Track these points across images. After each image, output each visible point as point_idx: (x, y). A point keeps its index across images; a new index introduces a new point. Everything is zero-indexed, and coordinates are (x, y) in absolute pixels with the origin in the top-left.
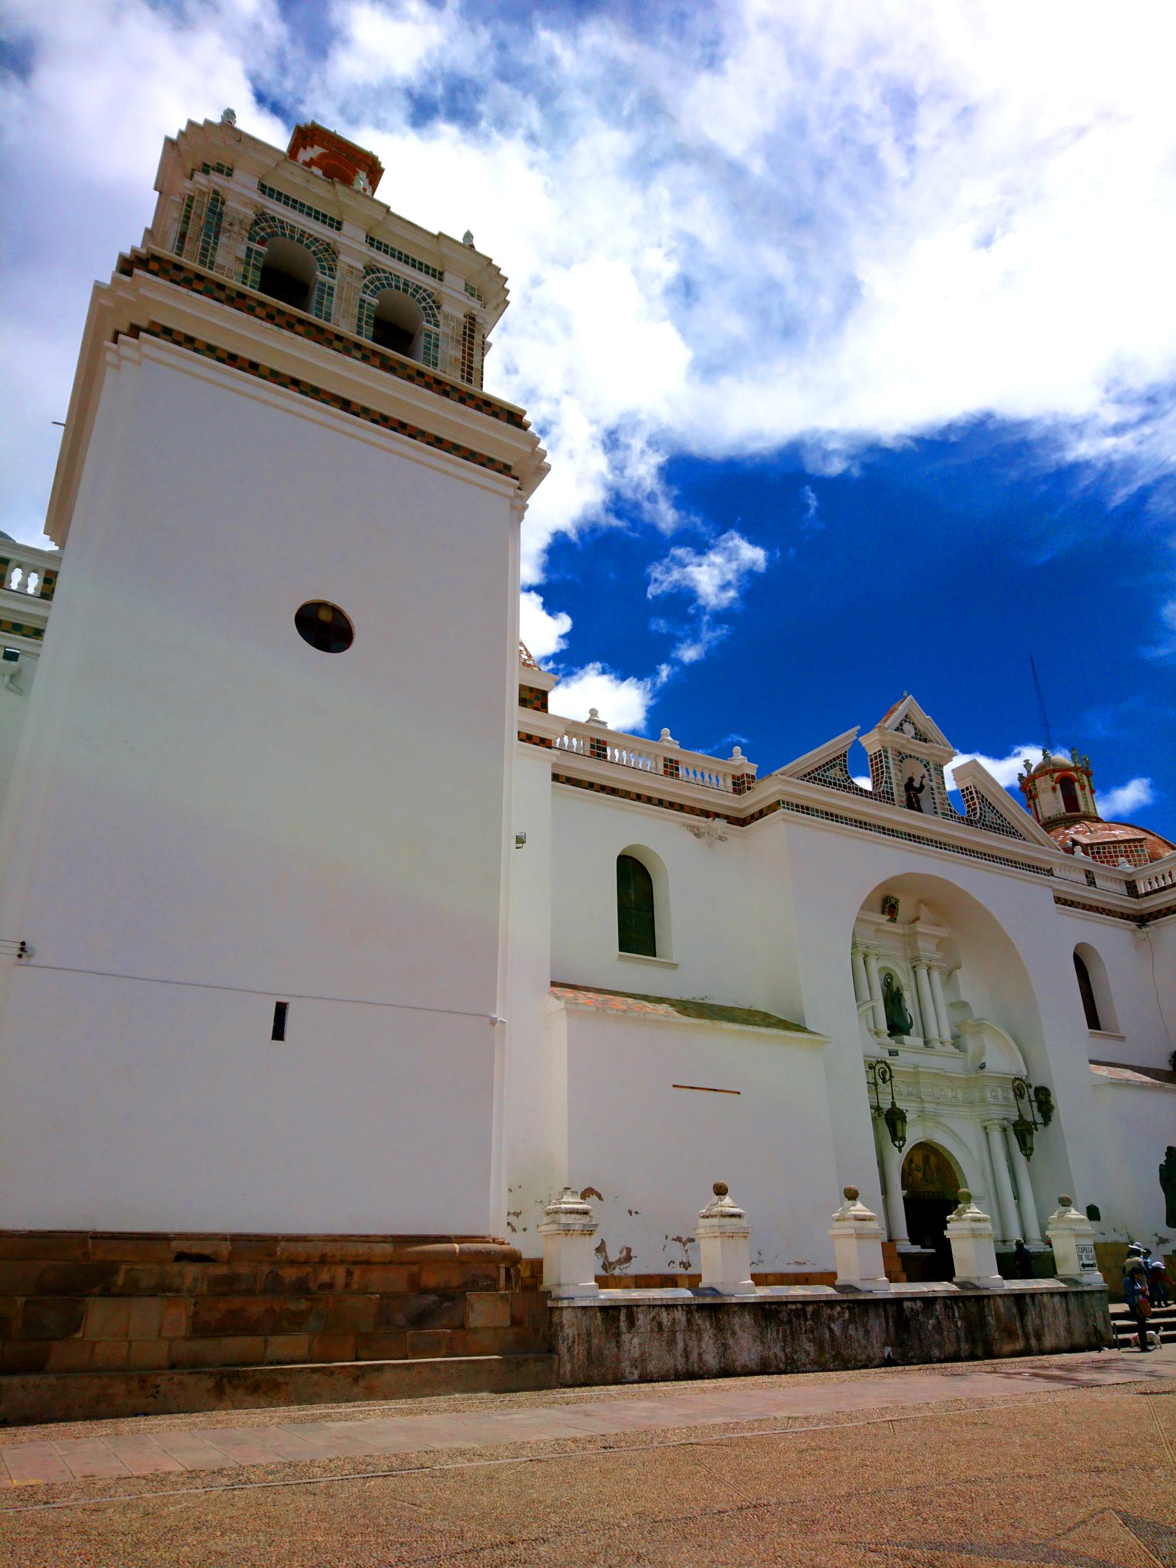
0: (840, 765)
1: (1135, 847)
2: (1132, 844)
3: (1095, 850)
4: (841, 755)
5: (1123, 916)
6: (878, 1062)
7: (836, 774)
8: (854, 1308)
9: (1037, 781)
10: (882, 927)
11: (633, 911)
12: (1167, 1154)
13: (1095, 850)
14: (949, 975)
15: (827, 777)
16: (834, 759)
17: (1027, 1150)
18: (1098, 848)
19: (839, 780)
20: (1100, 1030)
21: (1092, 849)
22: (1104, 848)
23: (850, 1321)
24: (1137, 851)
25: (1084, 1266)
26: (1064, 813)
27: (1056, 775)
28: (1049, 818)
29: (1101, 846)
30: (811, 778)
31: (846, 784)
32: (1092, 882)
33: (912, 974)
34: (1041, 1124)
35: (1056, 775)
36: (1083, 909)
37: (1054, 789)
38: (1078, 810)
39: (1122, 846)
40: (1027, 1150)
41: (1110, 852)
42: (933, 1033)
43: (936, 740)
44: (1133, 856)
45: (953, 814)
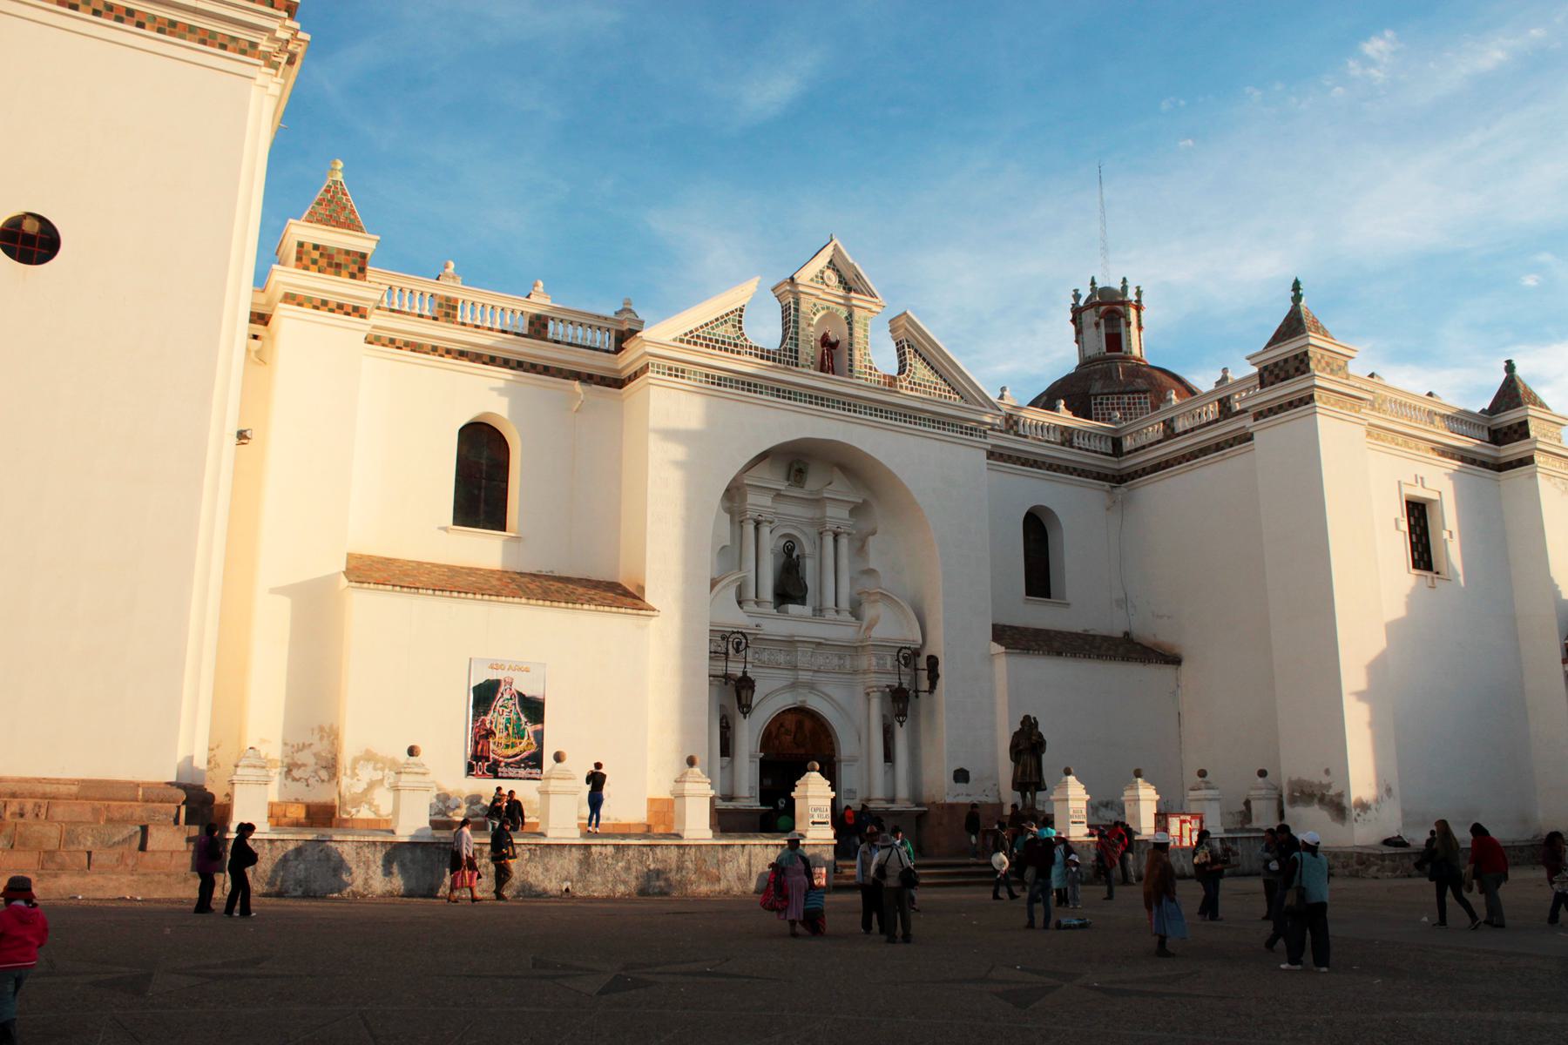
0: (734, 320)
1: (1140, 398)
2: (1136, 396)
3: (1099, 401)
4: (736, 310)
5: (1099, 476)
6: (733, 632)
7: (726, 331)
8: (535, 850)
9: (1083, 314)
10: (782, 493)
11: (484, 481)
12: (1022, 723)
13: (1099, 401)
15: (714, 335)
16: (727, 315)
18: (1102, 399)
19: (729, 338)
20: (1050, 598)
21: (1095, 399)
22: (1108, 399)
23: (529, 860)
24: (1140, 403)
26: (1104, 353)
27: (1103, 308)
28: (1089, 357)
29: (1105, 397)
30: (693, 337)
31: (737, 342)
34: (925, 691)
35: (1103, 308)
36: (1048, 470)
37: (1097, 325)
38: (1120, 349)
39: (1126, 397)
41: (1113, 404)
42: (830, 602)
43: (862, 291)
44: (1135, 409)
45: (873, 372)
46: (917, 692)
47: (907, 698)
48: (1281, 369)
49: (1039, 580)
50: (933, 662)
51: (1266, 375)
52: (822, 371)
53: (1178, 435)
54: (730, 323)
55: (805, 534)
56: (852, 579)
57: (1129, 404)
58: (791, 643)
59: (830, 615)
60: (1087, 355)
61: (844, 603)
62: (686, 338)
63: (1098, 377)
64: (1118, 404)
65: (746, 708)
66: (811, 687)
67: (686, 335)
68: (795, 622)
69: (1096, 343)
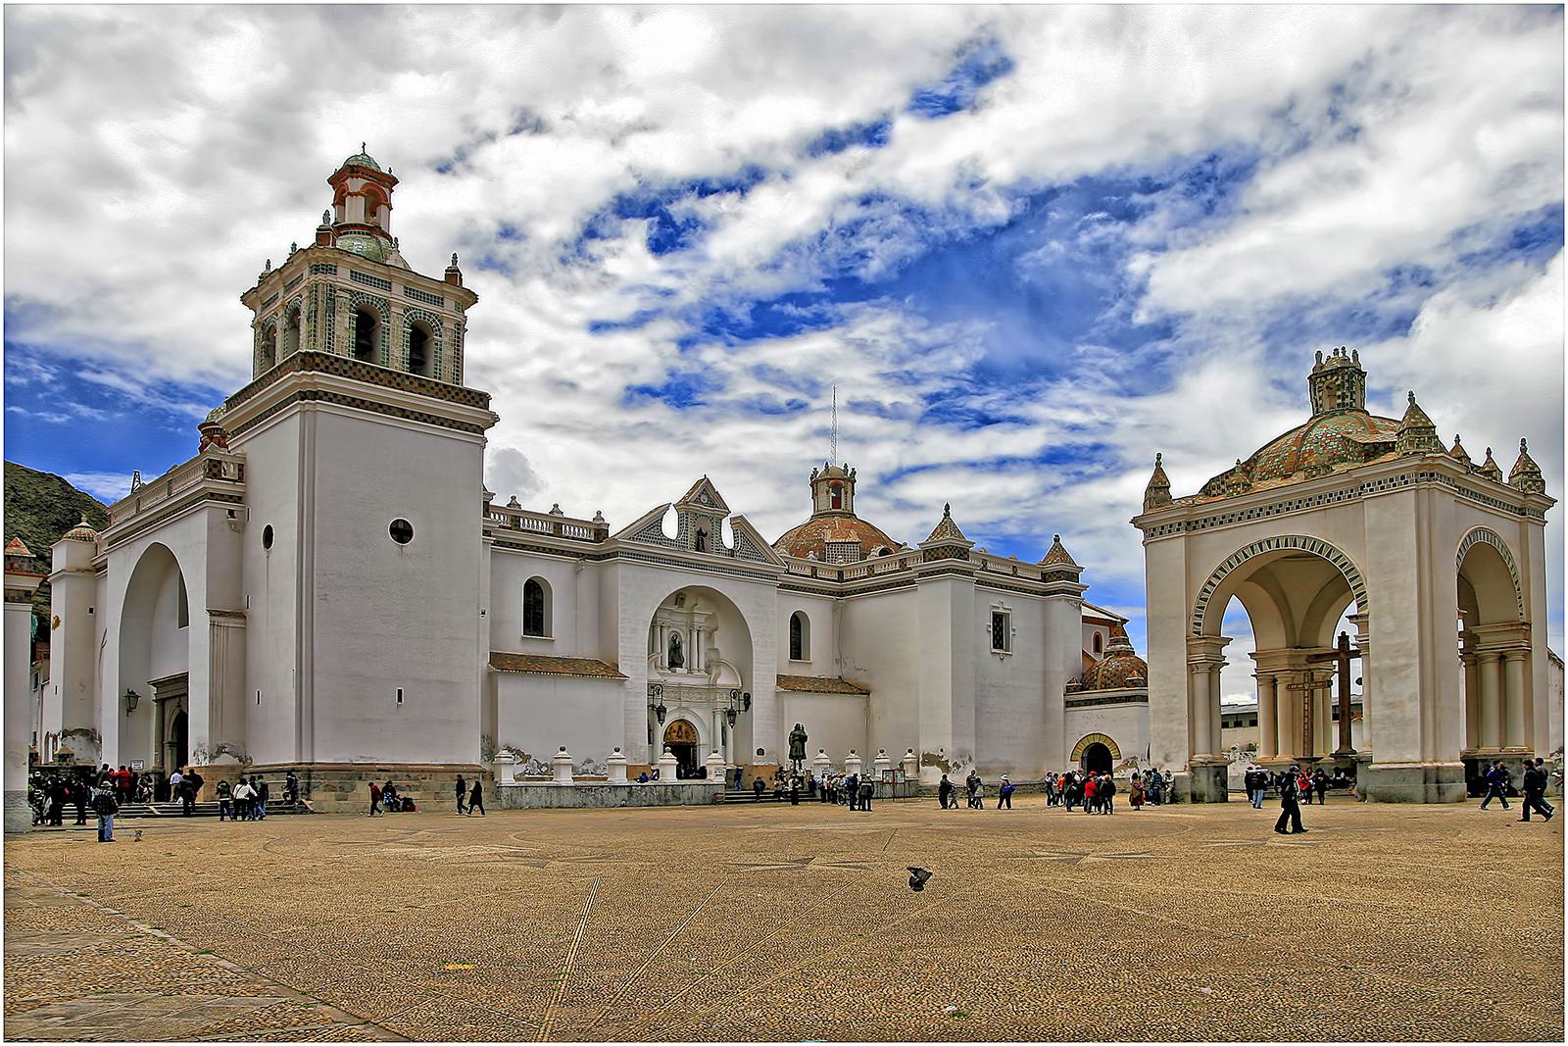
14: (710, 636)
17: (733, 722)
40: (733, 722)
46: (739, 711)
47: (735, 715)
49: (797, 651)
55: (683, 631)
56: (706, 654)
58: (680, 687)
59: (696, 673)
61: (702, 666)
65: (661, 720)
66: (687, 709)
68: (679, 677)
69: (826, 503)
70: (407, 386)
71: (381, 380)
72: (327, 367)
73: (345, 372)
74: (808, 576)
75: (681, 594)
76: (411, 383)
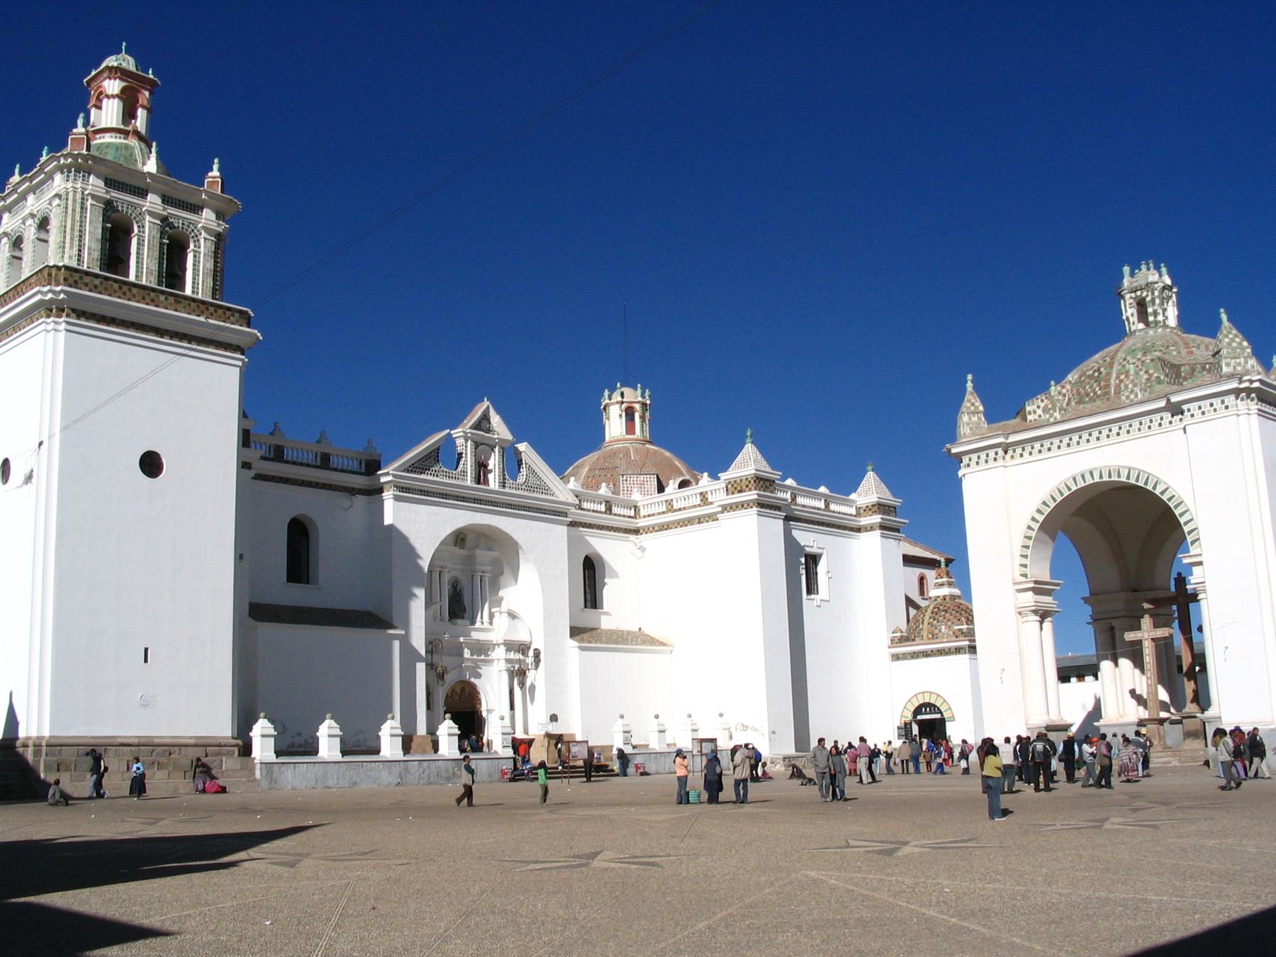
2: (648, 476)
13: (625, 478)
16: (431, 453)
21: (623, 477)
22: (630, 478)
25: (504, 747)
29: (629, 476)
32: (609, 509)
33: (470, 579)
38: (634, 433)
48: (738, 484)
50: (537, 654)
51: (730, 486)
52: (479, 483)
53: (676, 511)
54: (433, 458)
57: (643, 481)
60: (612, 435)
62: (410, 469)
63: (621, 456)
64: (637, 481)
67: (410, 467)
70: (162, 302)
71: (134, 296)
72: (76, 282)
73: (96, 287)
74: (601, 512)
75: (461, 533)
76: (166, 299)
